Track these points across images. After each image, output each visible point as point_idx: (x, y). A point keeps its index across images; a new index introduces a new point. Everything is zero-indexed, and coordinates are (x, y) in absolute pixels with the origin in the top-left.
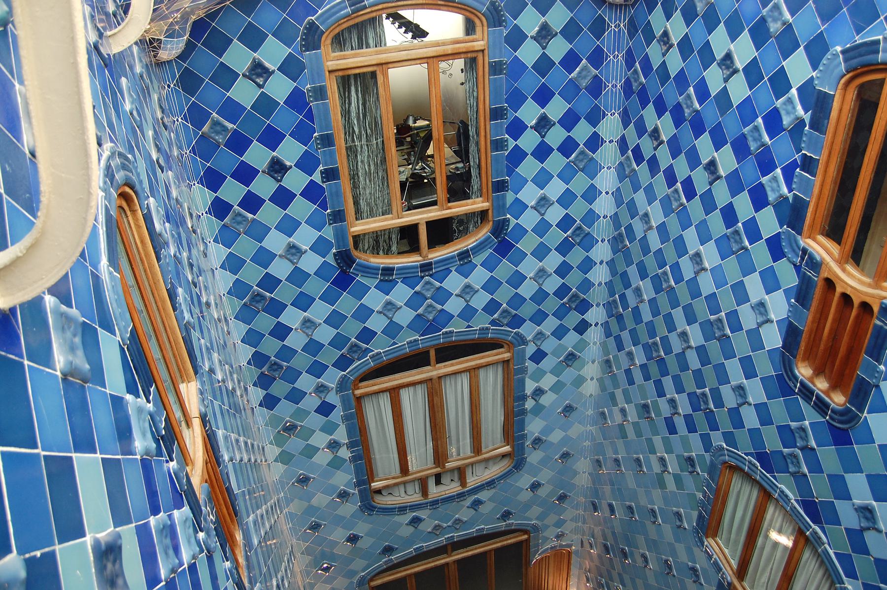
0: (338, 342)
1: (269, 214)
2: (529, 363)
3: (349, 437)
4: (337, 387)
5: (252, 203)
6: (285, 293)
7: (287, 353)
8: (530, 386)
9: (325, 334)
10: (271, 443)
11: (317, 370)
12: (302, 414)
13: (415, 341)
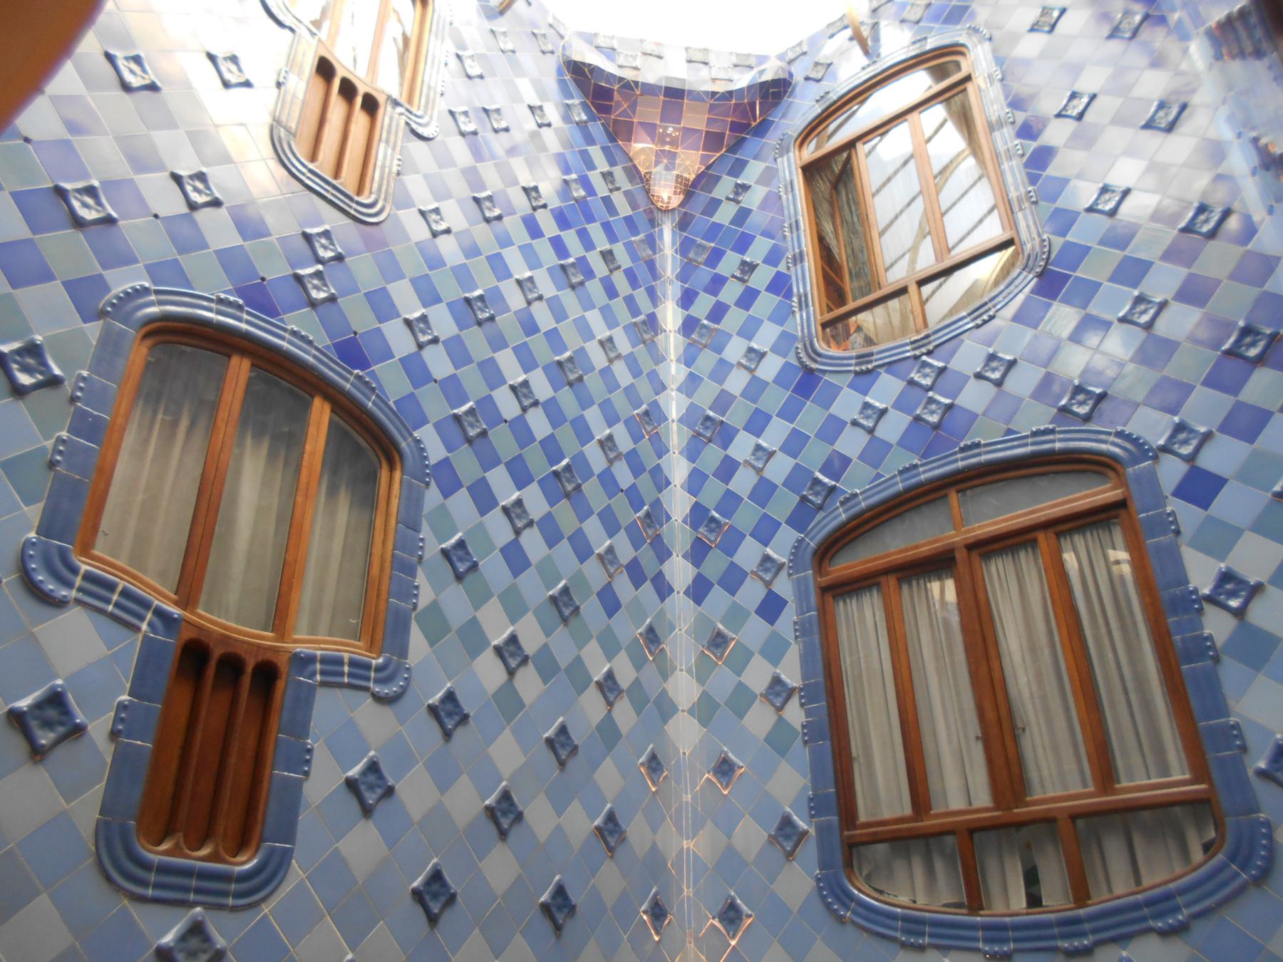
0: (797, 478)
1: (734, 318)
3: (805, 676)
4: (791, 561)
5: (718, 312)
6: (736, 416)
7: (730, 502)
8: (1201, 573)
9: (779, 469)
10: (689, 671)
11: (765, 531)
12: (736, 616)
13: (915, 467)
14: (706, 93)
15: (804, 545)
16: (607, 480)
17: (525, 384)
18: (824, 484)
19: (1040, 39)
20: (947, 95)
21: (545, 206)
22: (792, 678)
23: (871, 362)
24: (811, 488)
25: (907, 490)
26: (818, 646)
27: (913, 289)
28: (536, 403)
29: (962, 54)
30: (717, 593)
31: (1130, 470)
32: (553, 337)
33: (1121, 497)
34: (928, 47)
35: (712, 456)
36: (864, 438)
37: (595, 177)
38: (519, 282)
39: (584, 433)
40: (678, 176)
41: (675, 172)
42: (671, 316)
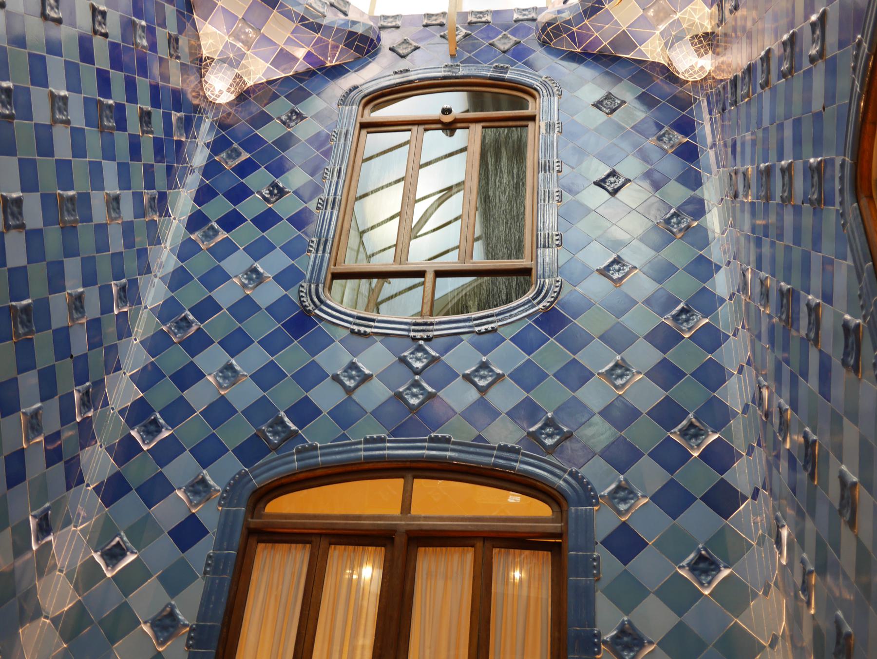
0: (260, 410)
2: (601, 552)
3: (202, 616)
4: (225, 491)
5: (231, 221)
6: (218, 326)
8: (608, 620)
9: (244, 394)
13: (382, 440)
14: (297, 14)
15: (246, 480)
16: (62, 339)
17: (18, 202)
18: (288, 427)
19: (600, 117)
20: (510, 123)
21: (106, 35)
22: (187, 616)
23: (370, 327)
24: (271, 426)
25: (368, 460)
26: (226, 588)
27: (430, 276)
28: (22, 226)
29: (534, 97)
30: (131, 501)
31: (573, 509)
32: (64, 168)
33: (559, 531)
34: (507, 76)
35: (175, 359)
36: (342, 396)
37: (161, 34)
38: (53, 97)
39: (56, 283)
40: (238, 76)
41: (237, 71)
42: (183, 202)
